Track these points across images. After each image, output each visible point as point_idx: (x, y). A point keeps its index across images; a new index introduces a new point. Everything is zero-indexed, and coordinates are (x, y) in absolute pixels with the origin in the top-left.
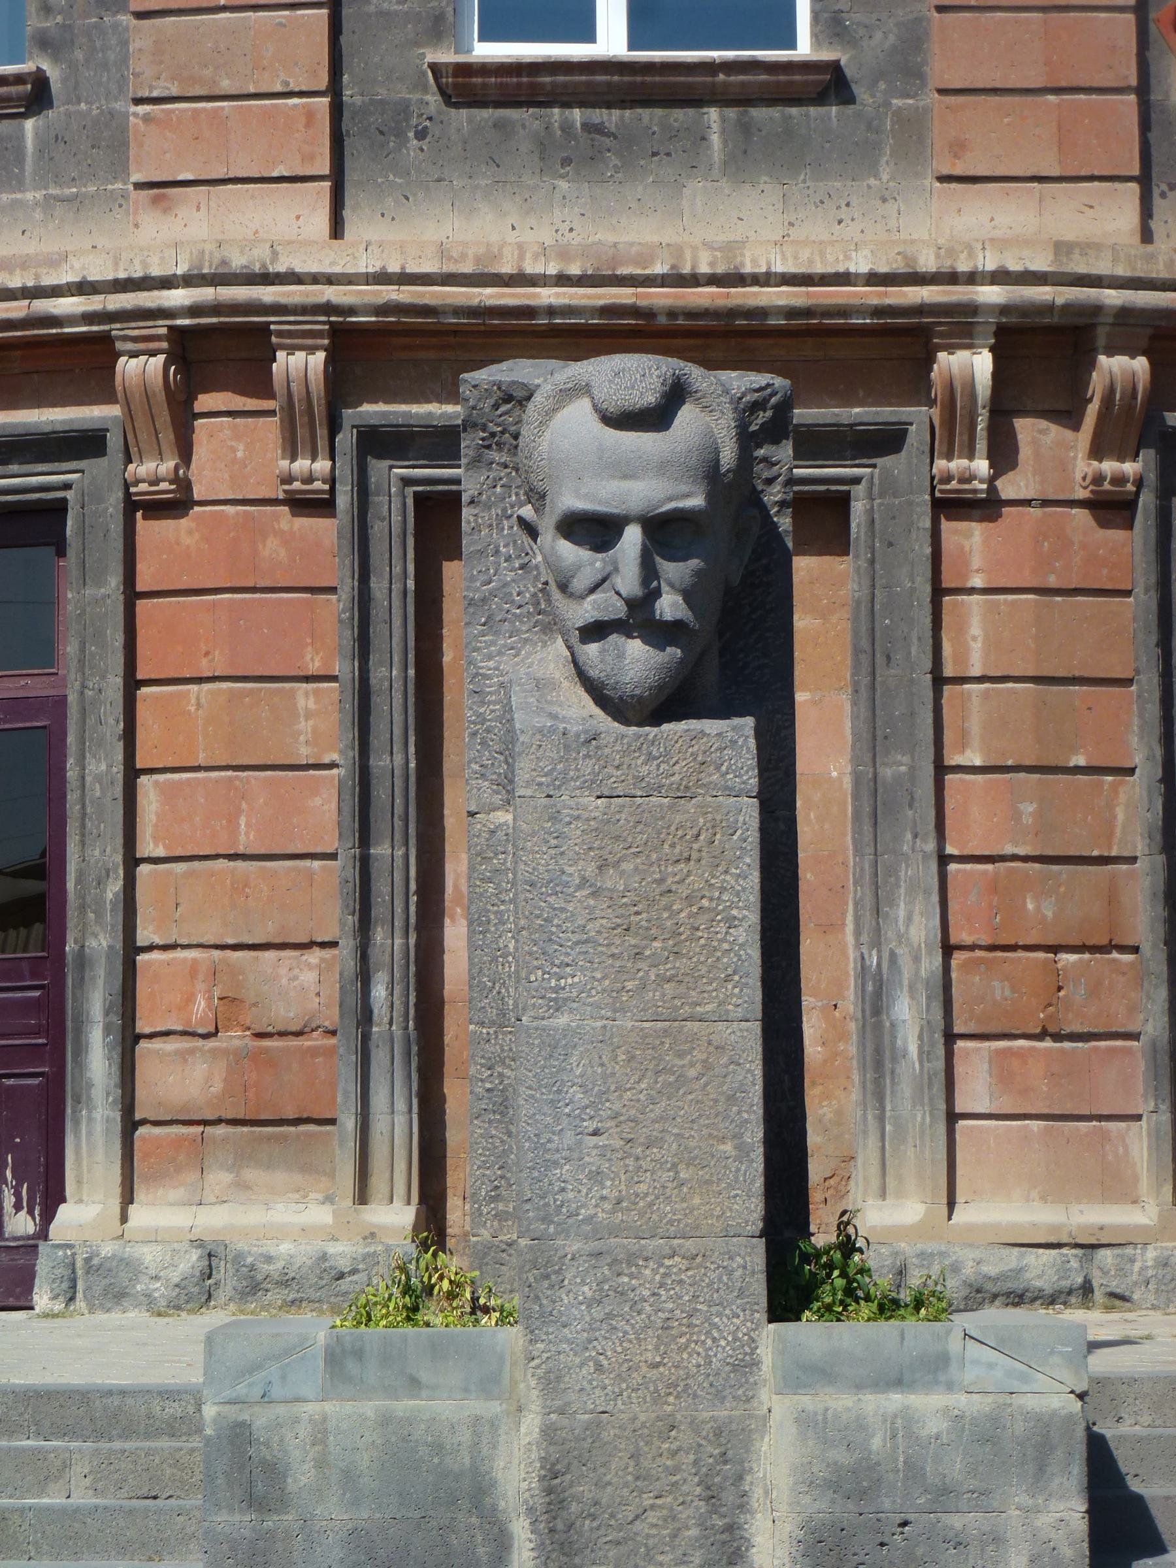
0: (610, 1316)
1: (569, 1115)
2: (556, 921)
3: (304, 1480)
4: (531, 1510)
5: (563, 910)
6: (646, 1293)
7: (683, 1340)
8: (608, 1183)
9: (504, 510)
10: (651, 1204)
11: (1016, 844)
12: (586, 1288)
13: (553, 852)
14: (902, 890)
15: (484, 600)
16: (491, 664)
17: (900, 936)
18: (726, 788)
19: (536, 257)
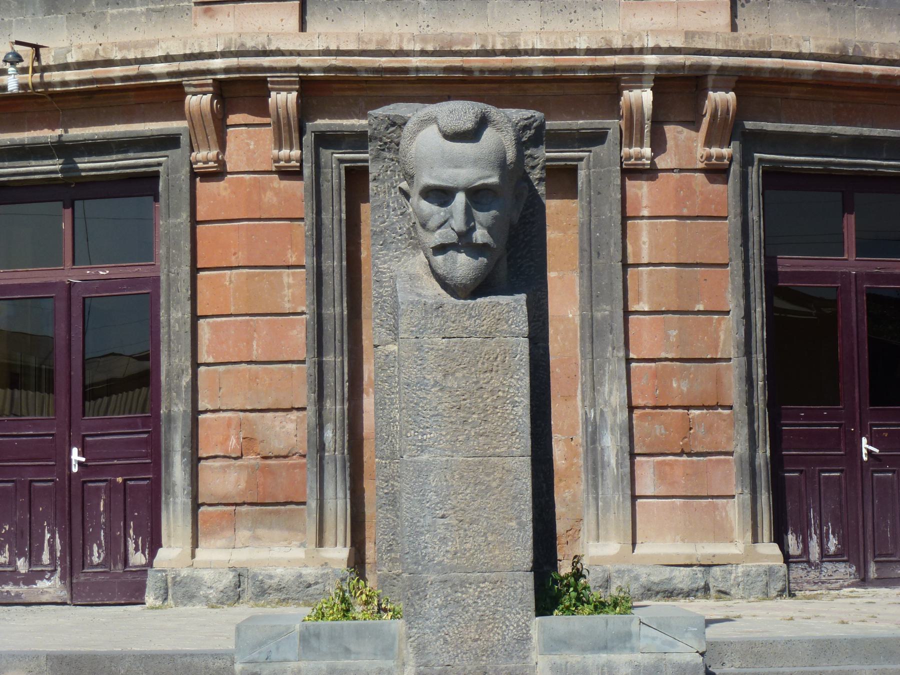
0: (451, 614)
5: (424, 398)
6: (470, 602)
7: (490, 626)
8: (450, 543)
9: (392, 183)
12: (438, 600)
13: (419, 367)
14: (607, 377)
15: (382, 232)
16: (386, 266)
17: (605, 402)
18: (512, 333)
19: (409, 41)
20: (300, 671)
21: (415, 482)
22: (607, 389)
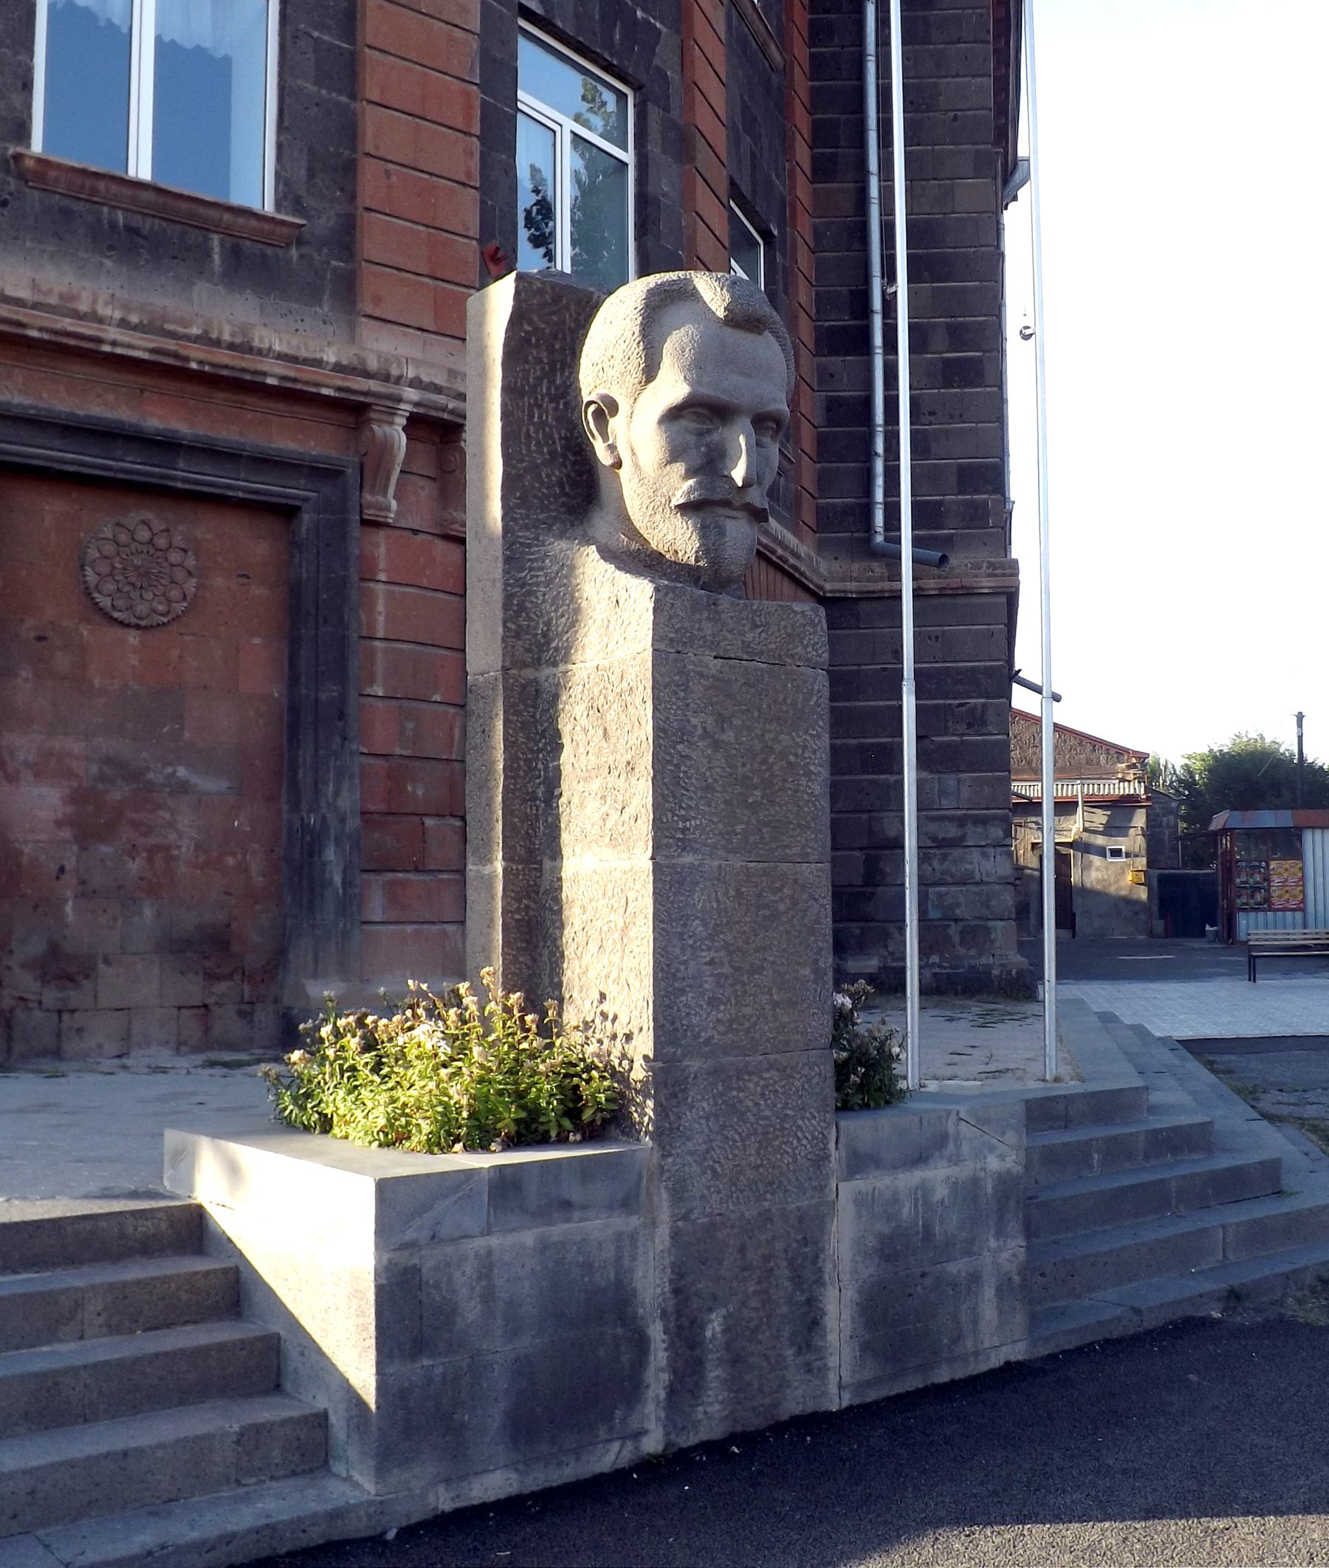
1: (692, 946)
2: (683, 768)
3: (471, 1317)
4: (664, 1314)
5: (688, 757)
6: (750, 1104)
8: (722, 1007)
10: (755, 1024)
11: (403, 748)
14: (332, 775)
17: (329, 805)
18: (809, 660)
19: (106, 303)
20: (490, 1253)
21: (673, 902)
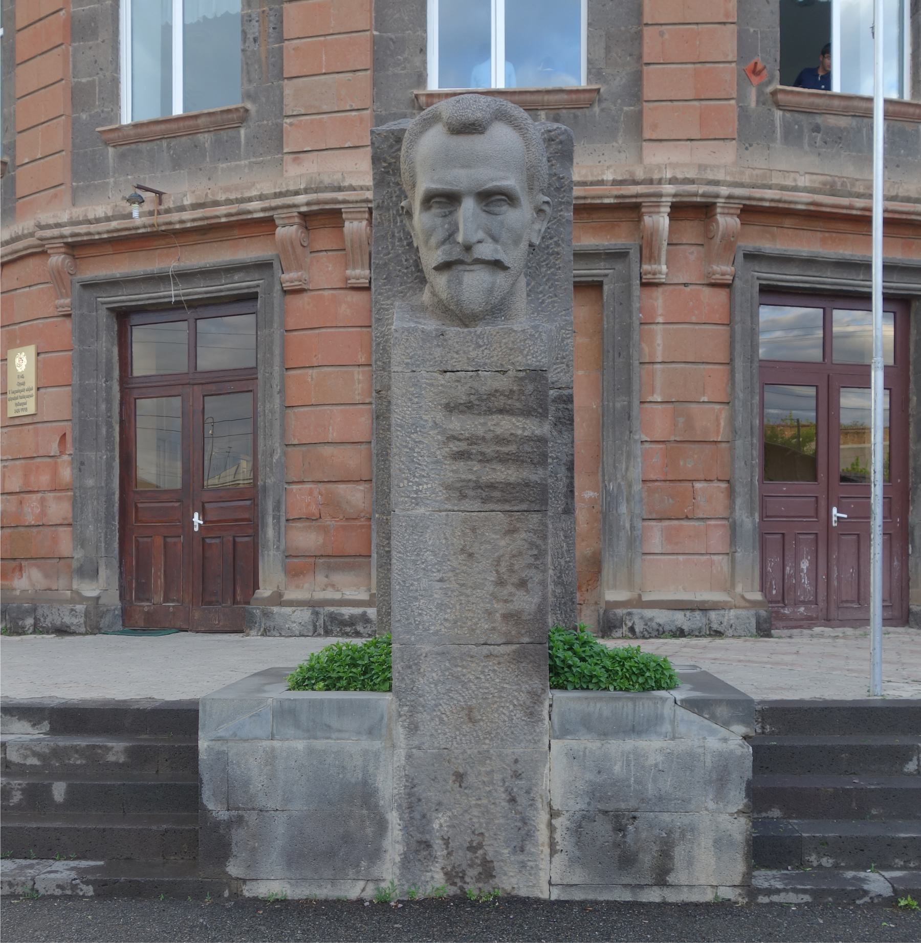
0: (450, 690)
1: (424, 569)
2: (416, 450)
5: (420, 442)
7: (495, 706)
8: (449, 611)
9: (398, 211)
12: (434, 675)
13: (415, 406)
15: (385, 264)
16: (389, 302)
20: (273, 749)
21: (408, 540)
22: (624, 466)
